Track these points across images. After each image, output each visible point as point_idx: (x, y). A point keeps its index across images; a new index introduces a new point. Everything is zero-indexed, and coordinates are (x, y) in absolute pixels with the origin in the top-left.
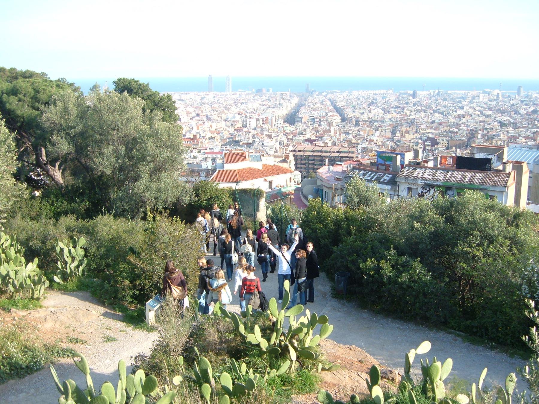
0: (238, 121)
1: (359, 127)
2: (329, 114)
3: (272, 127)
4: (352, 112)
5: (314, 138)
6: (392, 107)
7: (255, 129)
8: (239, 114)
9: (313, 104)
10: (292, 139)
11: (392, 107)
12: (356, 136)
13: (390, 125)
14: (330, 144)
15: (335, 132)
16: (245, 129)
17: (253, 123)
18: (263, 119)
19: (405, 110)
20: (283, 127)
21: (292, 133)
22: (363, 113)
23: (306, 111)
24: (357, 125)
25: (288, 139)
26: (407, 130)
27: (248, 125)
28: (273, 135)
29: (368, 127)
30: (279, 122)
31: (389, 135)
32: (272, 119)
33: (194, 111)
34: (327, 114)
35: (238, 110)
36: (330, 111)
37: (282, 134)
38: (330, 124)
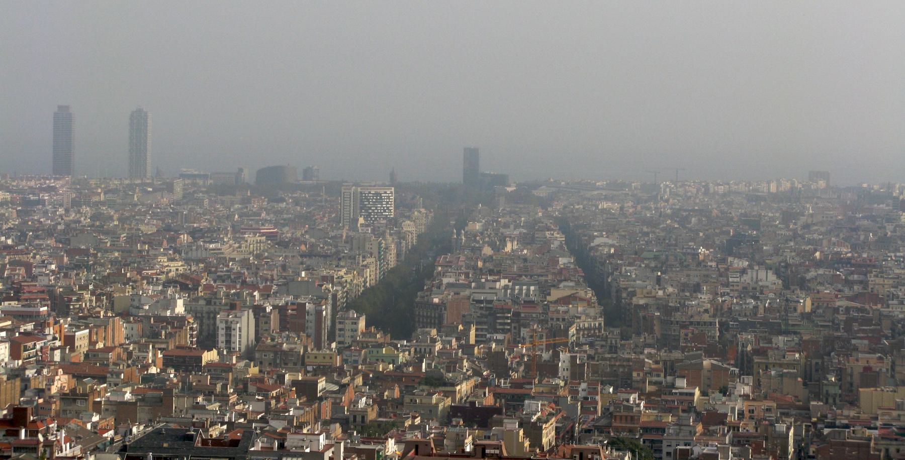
0: (181, 320)
1: (677, 355)
2: (555, 294)
3: (318, 346)
4: (649, 285)
5: (489, 400)
6: (818, 264)
7: (249, 355)
8: (184, 288)
9: (492, 245)
10: (398, 403)
11: (818, 264)
12: (657, 394)
13: (801, 346)
14: (548, 436)
15: (576, 373)
16: (210, 356)
17: (245, 328)
18: (282, 310)
19: (871, 278)
20: (364, 345)
21: (398, 376)
22: (697, 288)
23: (462, 279)
24: (666, 342)
25: (380, 402)
26: (867, 369)
27: (221, 339)
28: (322, 384)
29: (710, 353)
30: (348, 326)
31: (795, 389)
32: (319, 313)
34: (544, 290)
35: (176, 267)
36: (562, 275)
37: (359, 381)
38: (556, 335)
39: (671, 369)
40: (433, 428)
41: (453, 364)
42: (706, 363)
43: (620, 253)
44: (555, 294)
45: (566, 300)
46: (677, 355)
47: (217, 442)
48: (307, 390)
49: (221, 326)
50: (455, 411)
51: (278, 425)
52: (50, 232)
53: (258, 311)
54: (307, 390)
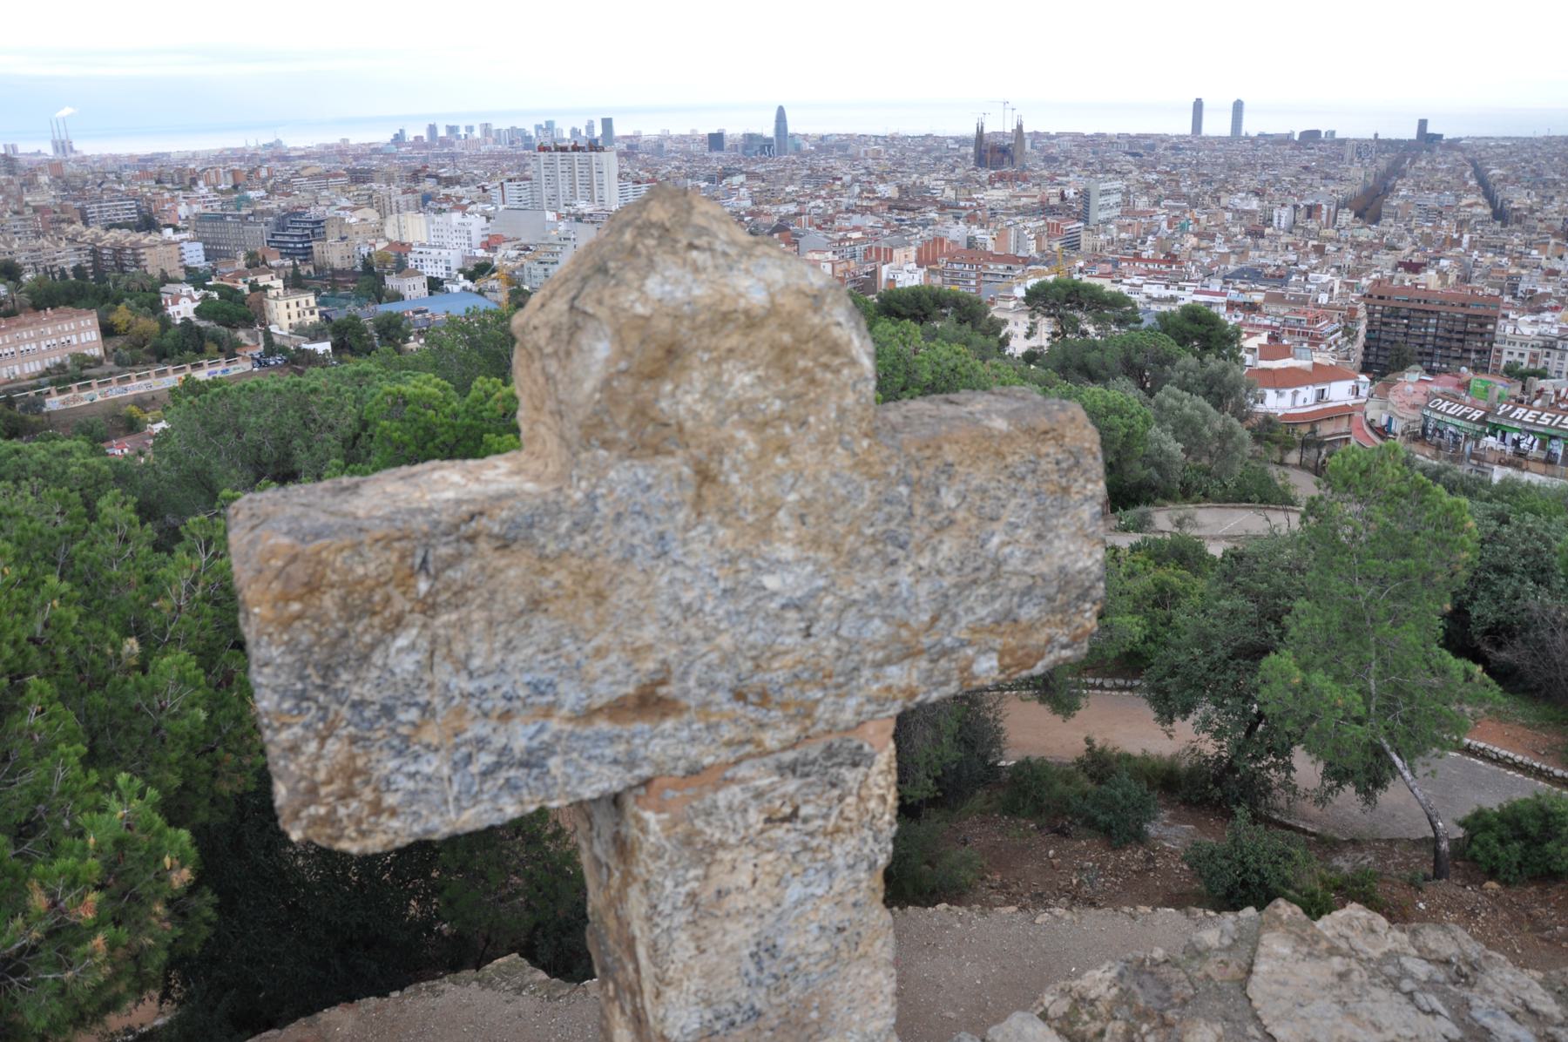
2: (1464, 202)
8: (1257, 194)
14: (1452, 279)
16: (1268, 231)
28: (1330, 248)
33: (1163, 183)
34: (1458, 197)
36: (1469, 191)
39: (1529, 244)
40: (1388, 273)
41: (1401, 238)
42: (1552, 241)
43: (1505, 179)
44: (1464, 202)
45: (1470, 206)
46: (1534, 236)
47: (1273, 276)
48: (1320, 250)
49: (1275, 214)
50: (1401, 264)
51: (1303, 267)
52: (1189, 164)
53: (1296, 207)
54: (1320, 250)
